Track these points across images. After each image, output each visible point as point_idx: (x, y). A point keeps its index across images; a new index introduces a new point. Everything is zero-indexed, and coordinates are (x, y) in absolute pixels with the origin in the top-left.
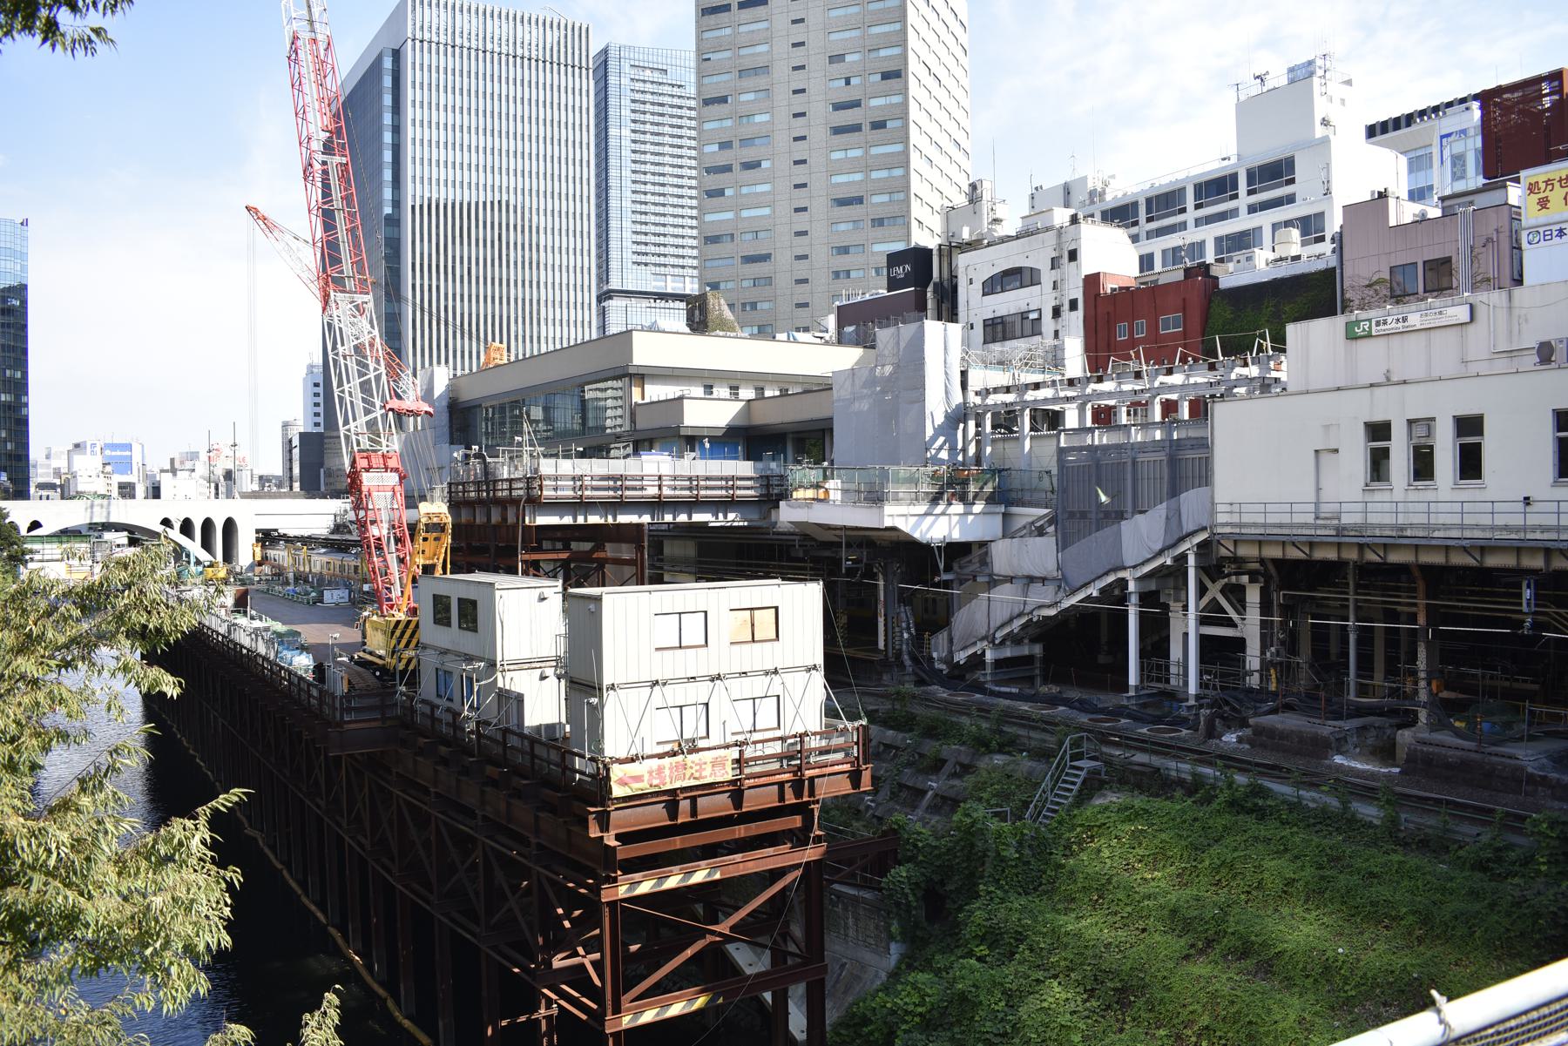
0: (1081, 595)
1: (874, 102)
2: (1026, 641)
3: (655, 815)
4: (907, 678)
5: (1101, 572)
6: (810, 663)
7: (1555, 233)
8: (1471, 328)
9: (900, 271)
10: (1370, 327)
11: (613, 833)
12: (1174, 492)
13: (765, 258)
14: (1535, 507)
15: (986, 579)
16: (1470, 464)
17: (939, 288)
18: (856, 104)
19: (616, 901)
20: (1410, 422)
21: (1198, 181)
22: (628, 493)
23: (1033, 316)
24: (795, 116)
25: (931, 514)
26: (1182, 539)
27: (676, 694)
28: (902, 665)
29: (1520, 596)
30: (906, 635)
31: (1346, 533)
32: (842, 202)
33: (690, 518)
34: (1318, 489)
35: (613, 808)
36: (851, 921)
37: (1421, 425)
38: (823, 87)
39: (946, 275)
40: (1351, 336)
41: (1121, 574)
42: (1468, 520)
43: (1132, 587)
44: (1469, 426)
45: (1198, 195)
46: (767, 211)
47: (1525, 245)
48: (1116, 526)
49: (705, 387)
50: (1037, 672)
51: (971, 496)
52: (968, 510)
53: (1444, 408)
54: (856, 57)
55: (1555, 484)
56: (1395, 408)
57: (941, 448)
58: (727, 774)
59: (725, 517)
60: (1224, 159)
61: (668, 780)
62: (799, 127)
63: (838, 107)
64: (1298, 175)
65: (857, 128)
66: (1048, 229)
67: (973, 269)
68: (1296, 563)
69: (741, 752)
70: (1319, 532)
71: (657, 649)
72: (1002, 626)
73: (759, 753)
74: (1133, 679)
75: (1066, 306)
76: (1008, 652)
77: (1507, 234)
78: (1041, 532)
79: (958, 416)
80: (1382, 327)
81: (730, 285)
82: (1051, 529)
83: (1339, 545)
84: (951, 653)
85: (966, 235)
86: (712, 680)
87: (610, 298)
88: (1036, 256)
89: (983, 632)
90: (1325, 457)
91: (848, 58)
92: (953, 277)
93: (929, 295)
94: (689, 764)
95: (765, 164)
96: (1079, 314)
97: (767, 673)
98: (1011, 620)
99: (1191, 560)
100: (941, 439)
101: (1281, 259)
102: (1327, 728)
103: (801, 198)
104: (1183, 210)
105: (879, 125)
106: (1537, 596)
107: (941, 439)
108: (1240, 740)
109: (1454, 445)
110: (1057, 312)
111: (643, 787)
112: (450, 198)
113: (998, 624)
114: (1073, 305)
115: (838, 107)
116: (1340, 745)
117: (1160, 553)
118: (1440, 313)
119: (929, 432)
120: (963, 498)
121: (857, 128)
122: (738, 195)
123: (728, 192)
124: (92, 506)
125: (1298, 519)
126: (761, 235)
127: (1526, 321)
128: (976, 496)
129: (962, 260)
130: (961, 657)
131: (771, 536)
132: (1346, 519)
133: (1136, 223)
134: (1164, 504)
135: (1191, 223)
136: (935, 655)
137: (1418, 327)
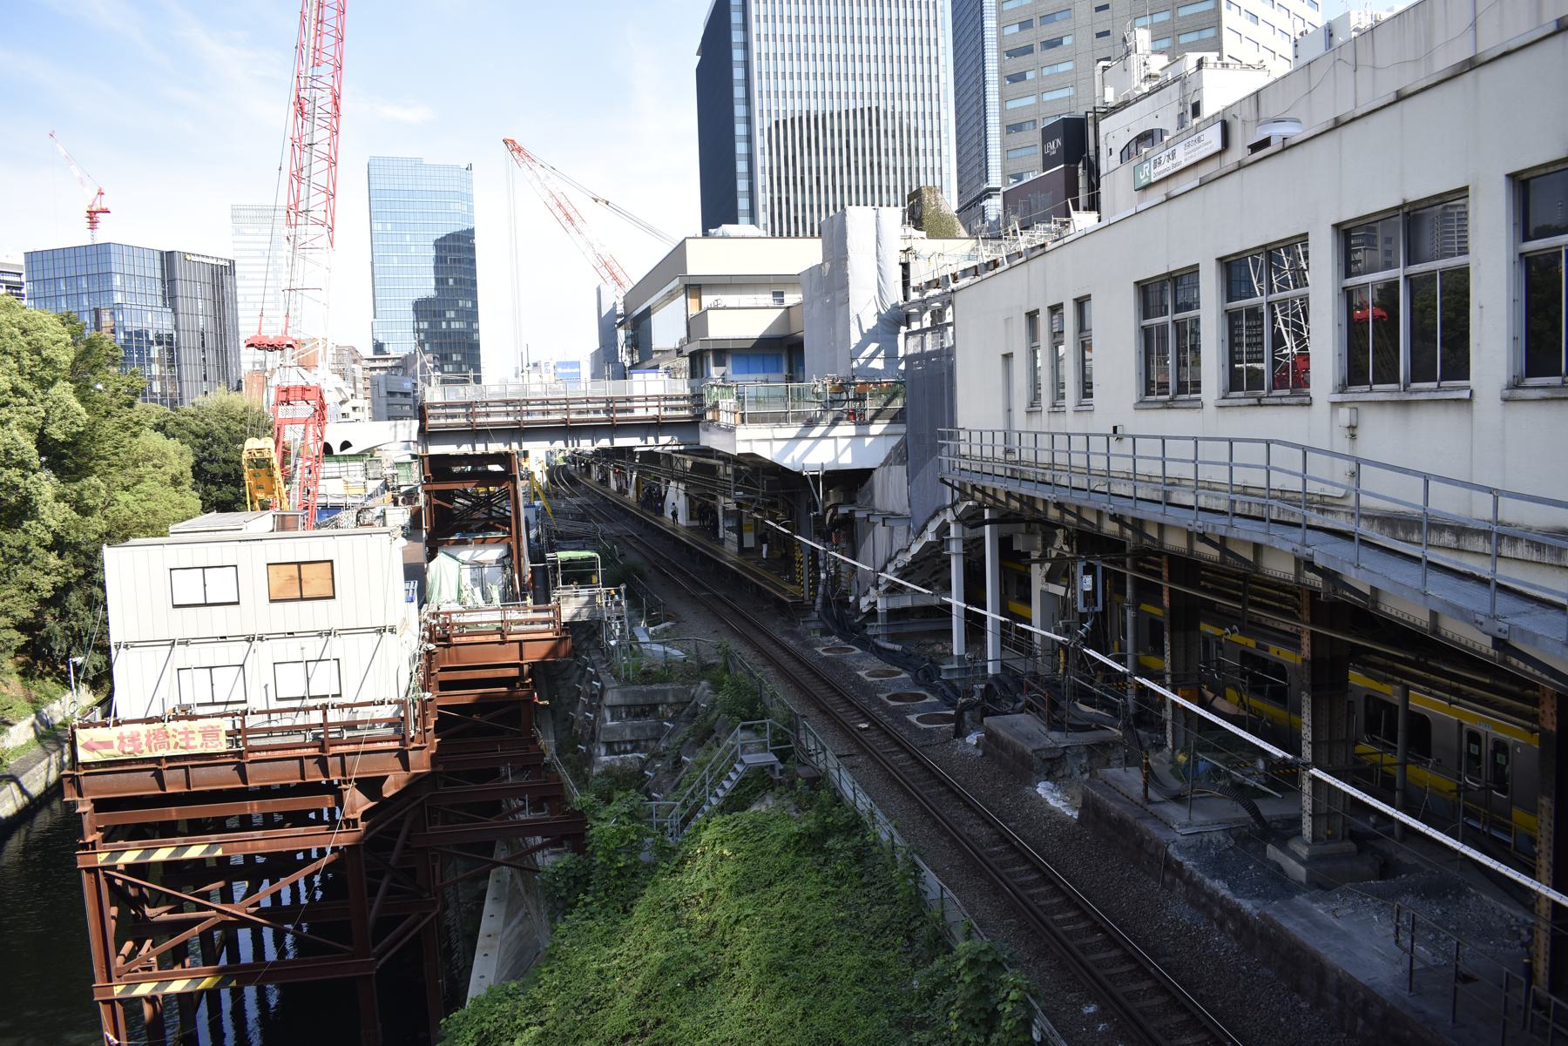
3: (143, 785)
4: (812, 625)
11: (88, 798)
19: (97, 868)
22: (618, 415)
25: (806, 438)
27: (182, 655)
30: (823, 576)
33: (612, 443)
35: (166, 766)
49: (775, 294)
51: (868, 415)
52: (863, 430)
55: (1141, 405)
57: (873, 357)
58: (221, 745)
59: (657, 441)
61: (144, 747)
79: (895, 320)
80: (1159, 169)
85: (1110, 97)
86: (248, 640)
87: (990, 197)
93: (1080, 171)
94: (171, 733)
95: (1066, 41)
97: (320, 635)
100: (873, 347)
107: (873, 347)
111: (113, 753)
118: (1199, 140)
119: (855, 338)
120: (857, 418)
122: (1042, 77)
123: (1030, 76)
124: (395, 426)
128: (878, 414)
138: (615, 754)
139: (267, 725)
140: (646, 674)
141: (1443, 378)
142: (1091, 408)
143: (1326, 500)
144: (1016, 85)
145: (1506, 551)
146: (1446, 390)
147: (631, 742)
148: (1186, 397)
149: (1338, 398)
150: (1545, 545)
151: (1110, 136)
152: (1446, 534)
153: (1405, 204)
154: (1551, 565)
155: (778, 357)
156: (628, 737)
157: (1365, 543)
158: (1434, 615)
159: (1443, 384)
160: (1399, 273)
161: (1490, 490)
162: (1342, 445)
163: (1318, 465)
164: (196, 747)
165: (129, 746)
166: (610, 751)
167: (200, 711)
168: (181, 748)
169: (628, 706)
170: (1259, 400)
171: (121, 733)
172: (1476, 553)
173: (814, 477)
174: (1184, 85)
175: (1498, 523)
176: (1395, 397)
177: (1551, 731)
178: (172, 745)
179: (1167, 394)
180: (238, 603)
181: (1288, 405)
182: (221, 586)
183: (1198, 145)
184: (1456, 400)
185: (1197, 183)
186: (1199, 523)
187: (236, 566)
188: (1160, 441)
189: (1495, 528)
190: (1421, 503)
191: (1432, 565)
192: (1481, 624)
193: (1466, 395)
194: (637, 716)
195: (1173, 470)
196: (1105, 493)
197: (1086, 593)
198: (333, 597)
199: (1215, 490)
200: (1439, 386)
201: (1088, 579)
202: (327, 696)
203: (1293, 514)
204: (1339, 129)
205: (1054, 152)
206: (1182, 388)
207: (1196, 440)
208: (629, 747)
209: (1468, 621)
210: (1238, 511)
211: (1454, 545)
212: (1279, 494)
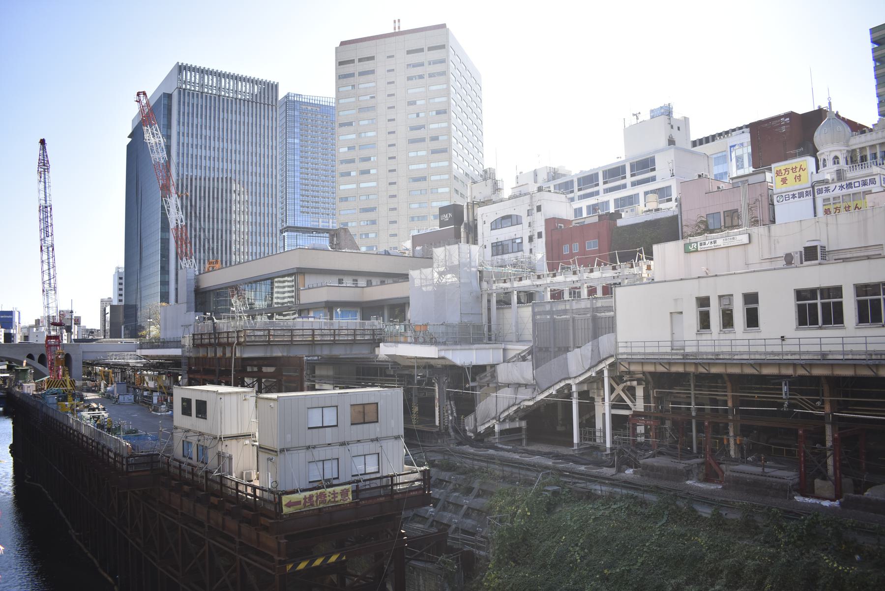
0: (546, 394)
1: (432, 126)
2: (517, 419)
5: (557, 381)
6: (396, 434)
7: (791, 197)
8: (750, 246)
9: (446, 217)
10: (697, 246)
12: (596, 336)
13: (373, 209)
14: (787, 342)
15: (495, 385)
16: (752, 320)
17: (467, 226)
20: (720, 297)
21: (604, 169)
23: (518, 241)
24: (389, 133)
26: (600, 362)
27: (320, 453)
28: (449, 435)
29: (781, 389)
30: (450, 418)
31: (688, 358)
32: (416, 180)
34: (673, 334)
36: (421, 581)
37: (724, 298)
39: (471, 219)
40: (687, 251)
41: (568, 382)
42: (753, 349)
43: (574, 388)
44: (751, 299)
45: (604, 177)
46: (374, 184)
47: (775, 203)
48: (564, 356)
50: (524, 436)
53: (738, 290)
56: (712, 290)
60: (618, 158)
62: (392, 139)
63: (413, 129)
64: (657, 166)
65: (423, 140)
66: (525, 194)
67: (485, 216)
68: (662, 374)
69: (357, 486)
70: (673, 357)
71: (309, 428)
72: (504, 411)
73: (368, 487)
74: (576, 440)
75: (536, 236)
76: (507, 426)
77: (766, 196)
78: (524, 359)
80: (703, 246)
81: (354, 224)
82: (530, 357)
83: (684, 364)
84: (476, 427)
88: (520, 209)
89: (493, 415)
90: (675, 316)
92: (475, 220)
93: (462, 230)
96: (543, 240)
97: (372, 440)
98: (509, 408)
99: (606, 373)
101: (649, 211)
102: (681, 465)
103: (393, 177)
104: (597, 185)
106: (790, 390)
108: (635, 473)
109: (743, 309)
110: (531, 239)
113: (502, 410)
114: (540, 235)
115: (413, 129)
116: (688, 474)
117: (589, 369)
121: (423, 140)
125: (662, 350)
126: (371, 197)
127: (778, 242)
129: (480, 211)
130: (481, 429)
131: (375, 363)
132: (688, 350)
133: (572, 192)
134: (590, 343)
135: (601, 192)
136: (467, 428)
137: (723, 246)
144: (345, 178)
155: (356, 312)
164: (337, 501)
171: (305, 496)
173: (468, 368)
174: (531, 198)
180: (337, 426)
182: (330, 417)
187: (337, 406)
198: (377, 422)
202: (357, 475)
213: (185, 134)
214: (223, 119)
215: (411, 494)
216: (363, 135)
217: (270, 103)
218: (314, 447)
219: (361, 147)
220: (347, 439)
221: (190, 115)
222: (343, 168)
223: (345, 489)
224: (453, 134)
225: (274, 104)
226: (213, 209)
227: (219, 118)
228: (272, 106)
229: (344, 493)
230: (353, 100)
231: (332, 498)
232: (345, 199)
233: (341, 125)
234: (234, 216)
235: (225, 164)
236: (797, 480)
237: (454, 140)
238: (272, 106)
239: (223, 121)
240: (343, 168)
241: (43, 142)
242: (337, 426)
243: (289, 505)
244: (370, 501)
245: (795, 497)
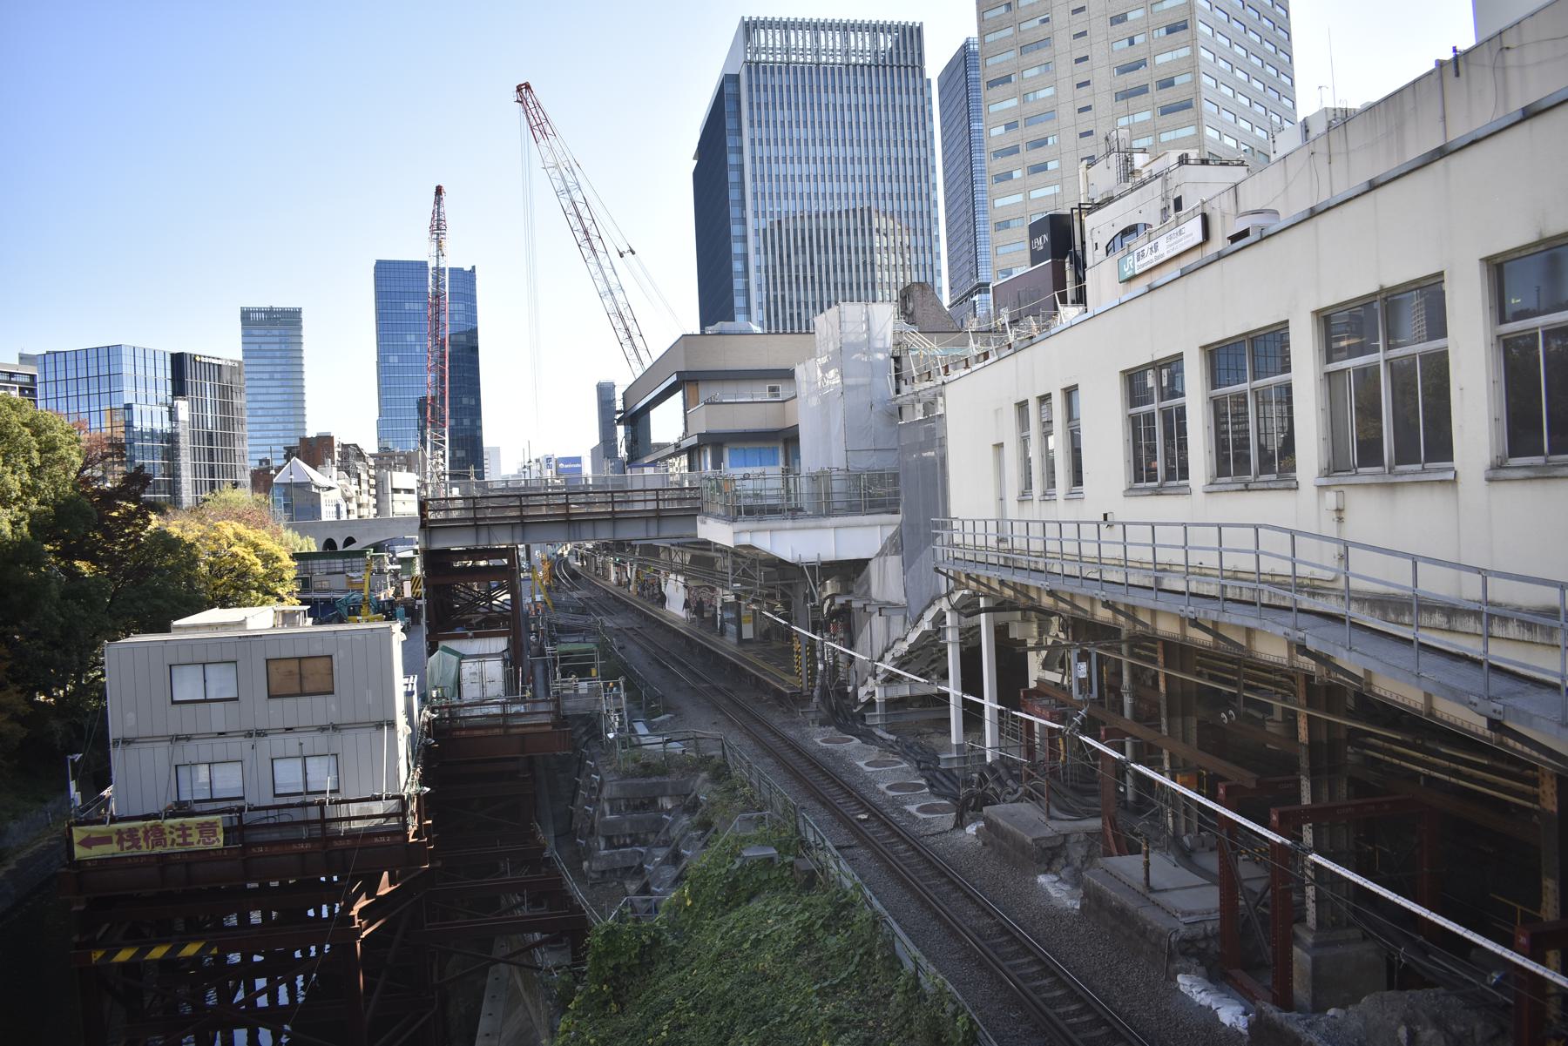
1: (1160, 59)
18: (1140, 64)
24: (1079, 86)
30: (820, 667)
38: (1106, 49)
46: (1057, 189)
54: (1139, 13)
55: (1130, 492)
63: (1124, 70)
65: (1143, 90)
69: (240, 818)
73: (271, 821)
80: (1142, 262)
91: (1131, 16)
93: (1067, 265)
97: (322, 729)
105: (1167, 83)
112: (814, 210)
115: (1124, 70)
118: (1180, 233)
121: (1143, 90)
129: (1089, 221)
138: (615, 847)
139: (265, 822)
140: (646, 766)
141: (1427, 460)
142: (1081, 496)
143: (1316, 583)
144: (1003, 184)
145: (1497, 630)
146: (1429, 471)
147: (630, 835)
148: (1174, 483)
149: (1324, 481)
150: (1536, 625)
151: (1095, 231)
152: (1437, 615)
153: (1382, 290)
154: (1543, 644)
155: (775, 450)
156: (628, 831)
157: (1356, 626)
158: (1428, 697)
159: (1428, 465)
160: (1379, 357)
161: (1479, 571)
162: (1330, 529)
163: (1306, 548)
164: (192, 843)
165: (128, 841)
166: (610, 845)
167: (197, 808)
168: (178, 845)
169: (628, 799)
170: (1246, 485)
172: (1467, 633)
175: (1488, 603)
176: (1380, 480)
177: (1552, 811)
178: (169, 842)
179: (1156, 480)
181: (1275, 489)
183: (1179, 238)
184: (1440, 481)
185: (1178, 273)
186: (1191, 609)
187: (235, 662)
188: (1150, 527)
189: (1485, 608)
190: (1411, 585)
191: (1424, 647)
192: (1475, 705)
193: (1450, 476)
194: (636, 809)
195: (1164, 556)
196: (1097, 580)
197: (1081, 681)
198: (332, 693)
199: (1206, 575)
200: (1423, 468)
201: (1083, 666)
203: (1284, 598)
204: (1315, 219)
205: (1041, 248)
206: (1170, 475)
207: (1185, 525)
208: (628, 841)
209: (1462, 702)
210: (1229, 596)
211: (1445, 626)
212: (1269, 578)
213: (764, 140)
214: (827, 105)
215: (376, 840)
216: (1031, 96)
217: (909, 63)
218: (188, 738)
219: (1029, 121)
220: (261, 726)
221: (770, 107)
222: (999, 165)
223: (207, 823)
224: (1203, 67)
225: (916, 63)
226: (820, 267)
227: (820, 105)
228: (914, 67)
229: (202, 828)
230: (1009, 31)
231: (179, 836)
232: (1003, 225)
233: (992, 84)
234: (878, 275)
235: (828, 184)
236: (1212, 926)
237: (1206, 80)
238: (914, 67)
239: (827, 109)
240: (999, 165)
241: (439, 190)
242: (236, 699)
243: (87, 843)
244: (276, 849)
245: (1180, 978)
